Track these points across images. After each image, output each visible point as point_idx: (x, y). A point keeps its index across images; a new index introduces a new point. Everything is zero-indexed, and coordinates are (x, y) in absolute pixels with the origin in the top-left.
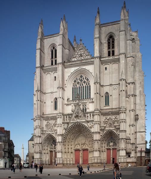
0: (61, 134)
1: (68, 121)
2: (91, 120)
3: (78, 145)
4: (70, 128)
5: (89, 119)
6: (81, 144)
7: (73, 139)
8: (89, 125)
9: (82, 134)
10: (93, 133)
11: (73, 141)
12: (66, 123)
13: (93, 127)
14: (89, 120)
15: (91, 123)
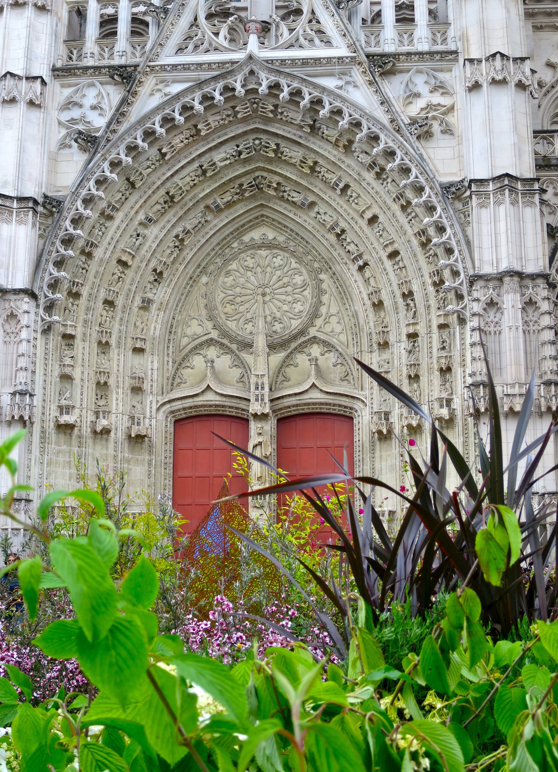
0: (31, 191)
1: (122, 50)
2: (424, 47)
3: (212, 352)
4: (149, 134)
5: (389, 39)
6: (261, 343)
7: (158, 276)
8: (398, 106)
9: (281, 227)
10: (457, 193)
11: (161, 294)
12: (97, 68)
13: (448, 131)
14: (390, 48)
15: (420, 84)
